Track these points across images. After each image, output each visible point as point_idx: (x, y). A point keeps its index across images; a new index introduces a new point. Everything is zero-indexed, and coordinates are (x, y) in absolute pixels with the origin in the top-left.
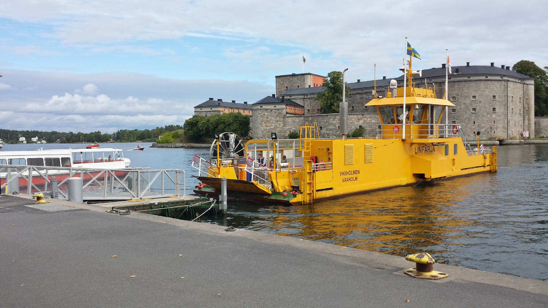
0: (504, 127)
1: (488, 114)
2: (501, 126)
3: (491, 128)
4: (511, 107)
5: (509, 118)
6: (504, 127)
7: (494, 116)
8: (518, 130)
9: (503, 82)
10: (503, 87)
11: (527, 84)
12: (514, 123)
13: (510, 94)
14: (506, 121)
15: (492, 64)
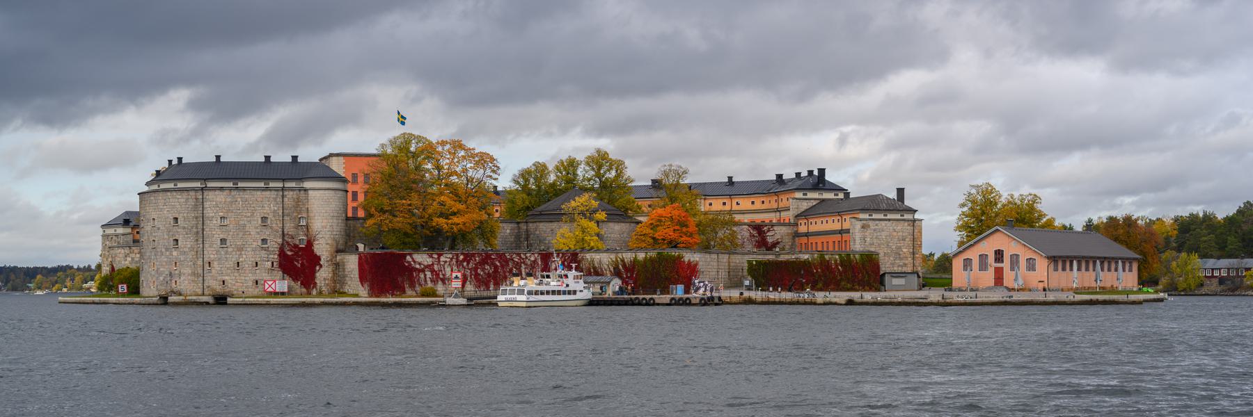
0: (193, 274)
1: (167, 250)
2: (188, 271)
3: (170, 274)
4: (218, 235)
5: (210, 254)
6: (193, 274)
7: (175, 253)
8: (251, 278)
9: (192, 193)
10: (191, 202)
11: (306, 190)
12: (231, 264)
13: (209, 213)
14: (200, 262)
15: (218, 157)
